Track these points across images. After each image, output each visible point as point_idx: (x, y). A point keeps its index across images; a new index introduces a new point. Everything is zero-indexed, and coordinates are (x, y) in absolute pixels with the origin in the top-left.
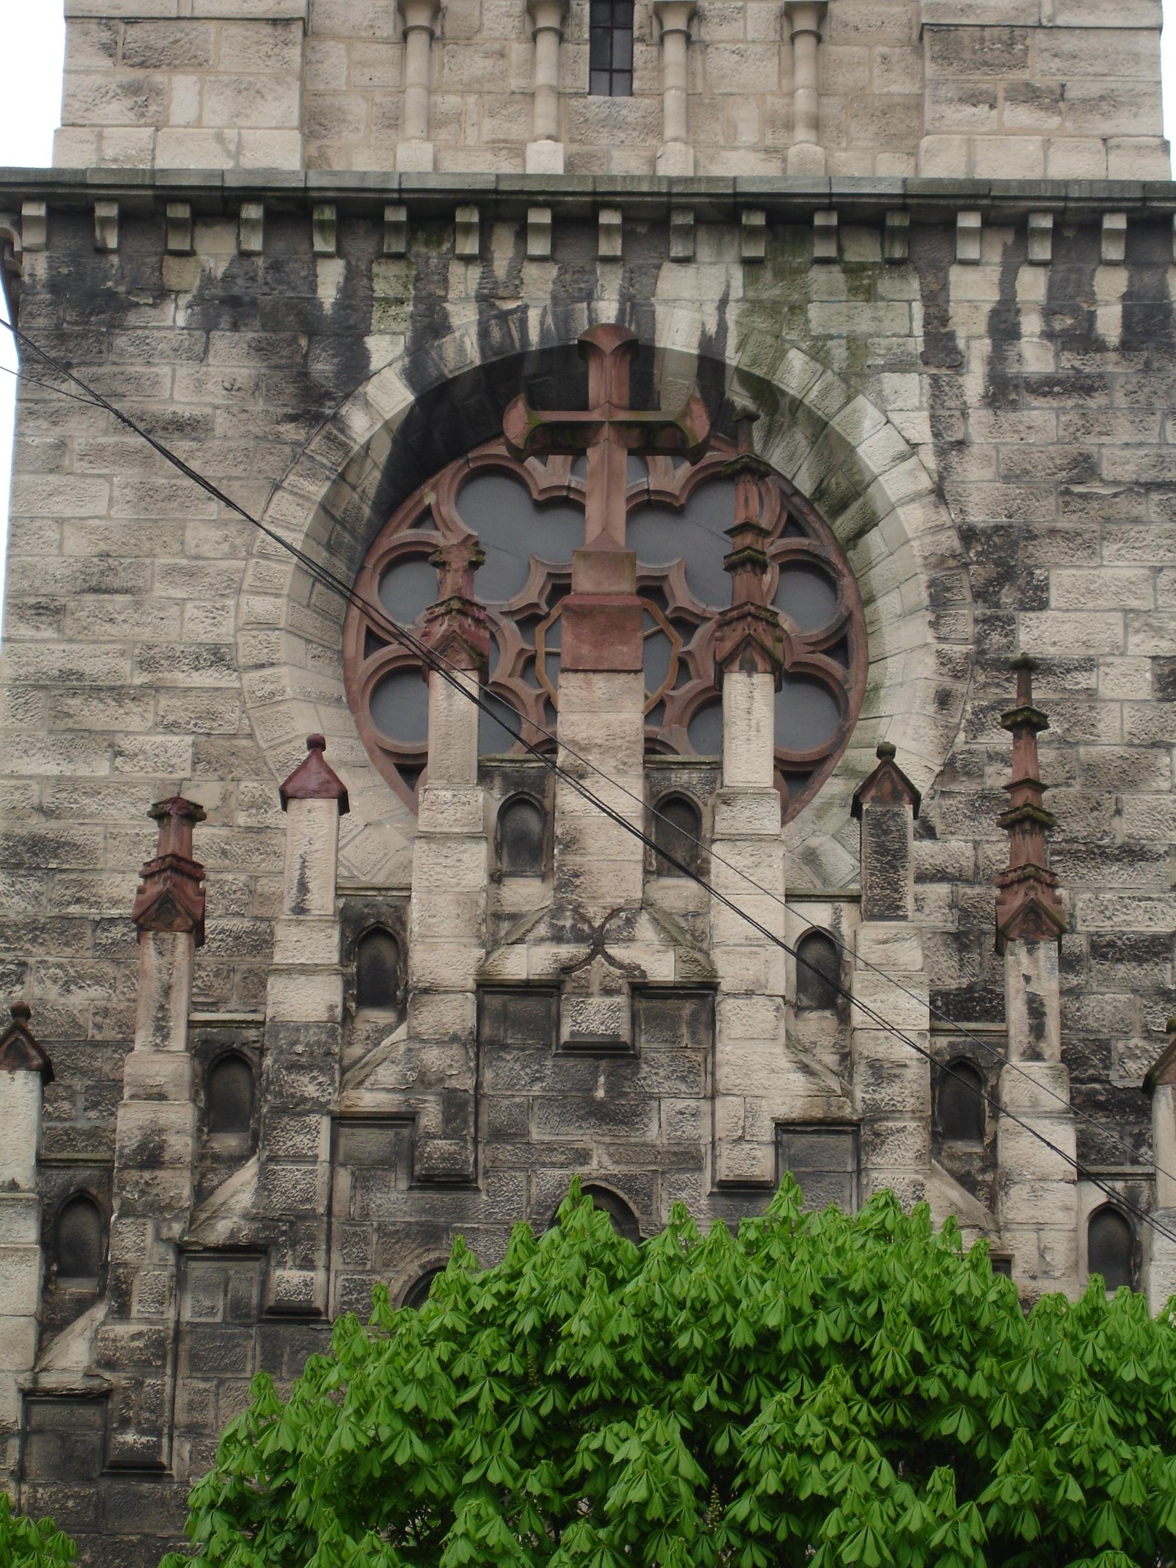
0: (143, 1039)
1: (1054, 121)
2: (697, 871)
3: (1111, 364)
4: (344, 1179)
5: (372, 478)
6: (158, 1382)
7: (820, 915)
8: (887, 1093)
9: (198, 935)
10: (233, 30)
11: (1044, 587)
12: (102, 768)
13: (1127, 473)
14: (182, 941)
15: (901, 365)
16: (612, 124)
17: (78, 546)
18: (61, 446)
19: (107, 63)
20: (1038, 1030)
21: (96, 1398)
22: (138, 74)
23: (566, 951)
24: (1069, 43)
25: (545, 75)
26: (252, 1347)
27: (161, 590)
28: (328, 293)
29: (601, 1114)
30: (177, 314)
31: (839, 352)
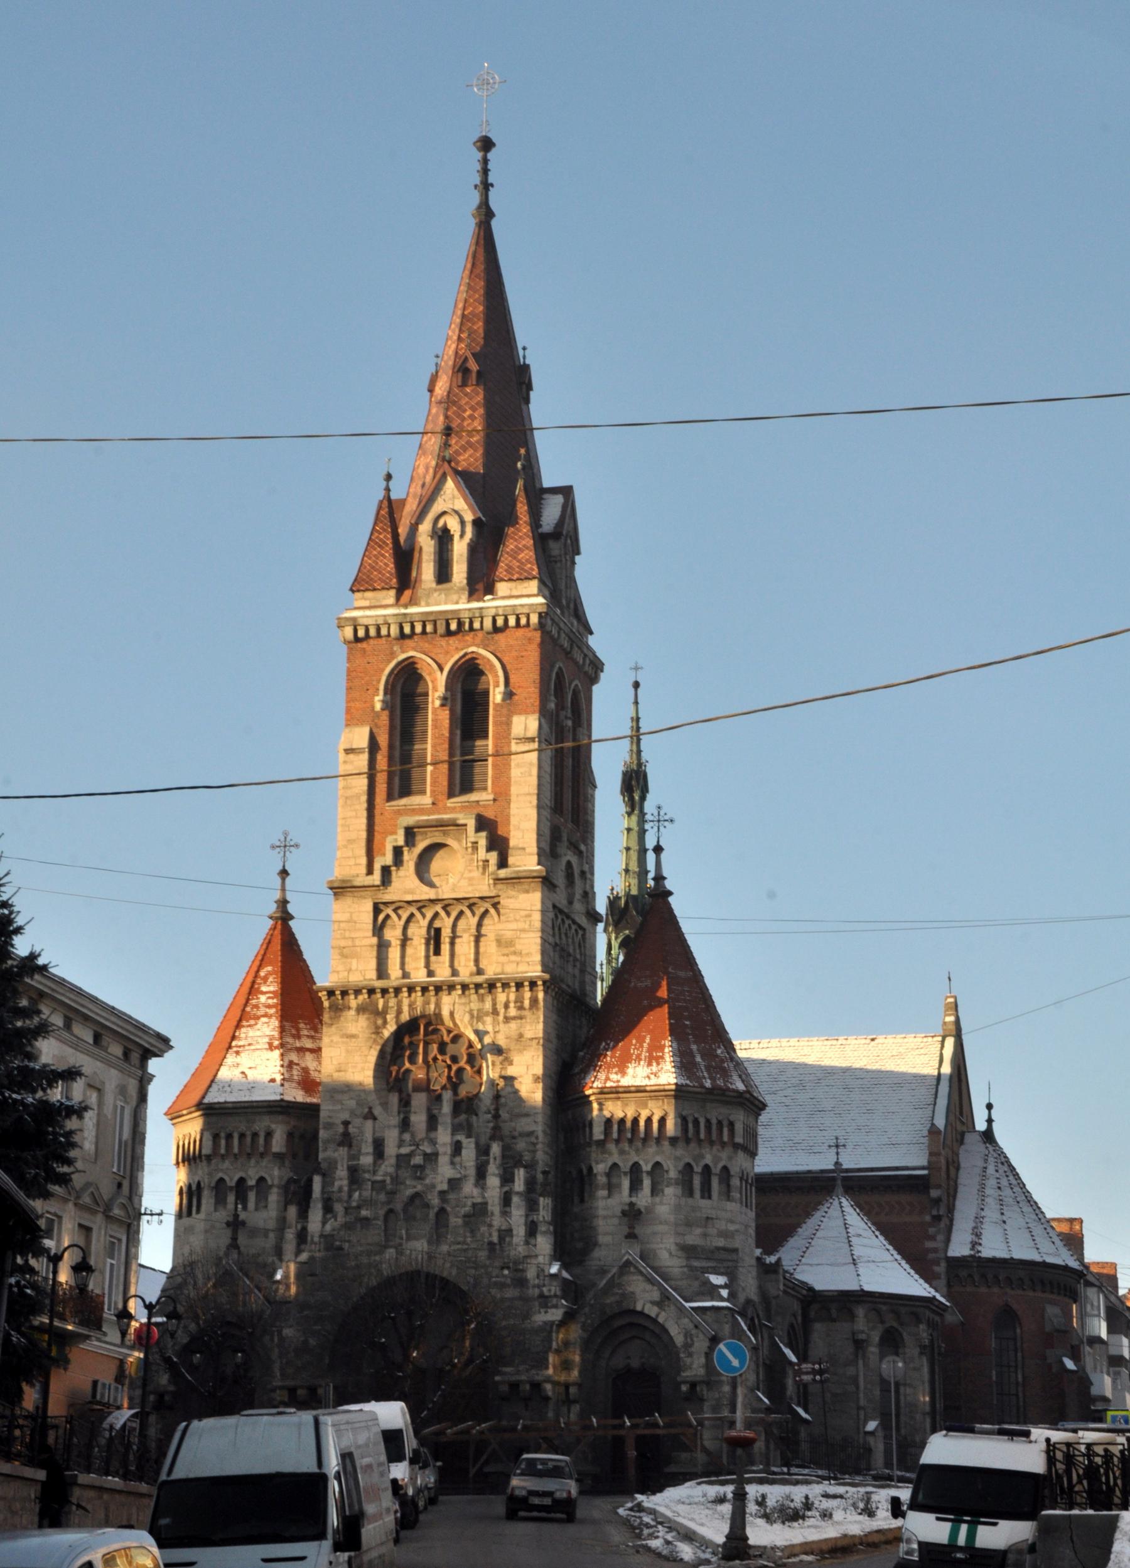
0: (339, 1167)
1: (518, 959)
2: (436, 1129)
3: (526, 1013)
4: (374, 1193)
5: (391, 1044)
6: (342, 1233)
7: (459, 1137)
8: (468, 1172)
9: (350, 1146)
10: (363, 948)
11: (512, 1061)
12: (339, 1107)
13: (529, 1036)
14: (346, 1149)
15: (487, 1014)
16: (439, 963)
17: (335, 1062)
18: (332, 1041)
19: (339, 957)
20: (495, 1159)
21: (333, 1236)
22: (344, 960)
23: (413, 1148)
24: (522, 941)
25: (423, 953)
26: (359, 1225)
27: (350, 1070)
28: (380, 1006)
29: (420, 1178)
30: (352, 1012)
31: (475, 1013)
